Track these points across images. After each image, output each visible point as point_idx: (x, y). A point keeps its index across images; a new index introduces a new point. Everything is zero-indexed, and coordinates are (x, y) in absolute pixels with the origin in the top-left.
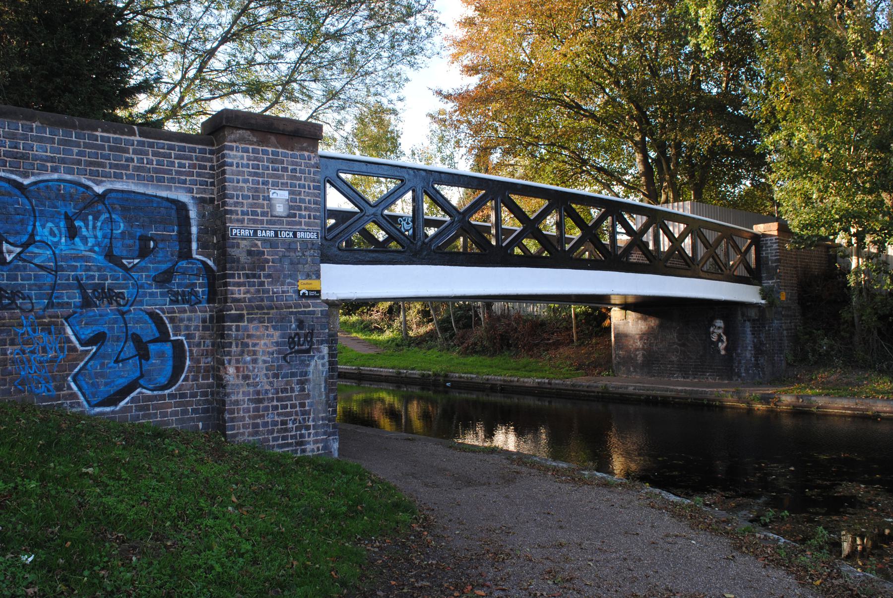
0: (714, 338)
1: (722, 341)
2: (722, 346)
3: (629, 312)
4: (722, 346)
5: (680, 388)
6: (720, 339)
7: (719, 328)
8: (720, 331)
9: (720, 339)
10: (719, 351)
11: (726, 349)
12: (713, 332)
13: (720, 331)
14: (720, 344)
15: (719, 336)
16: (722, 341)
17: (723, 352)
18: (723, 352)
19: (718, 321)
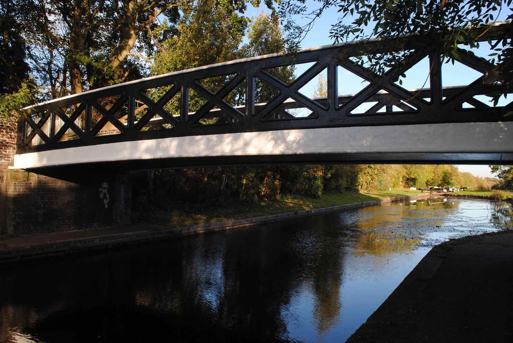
0: (101, 196)
1: (106, 198)
2: (106, 201)
3: (32, 174)
4: (106, 201)
5: (131, 233)
6: (105, 197)
7: (105, 188)
8: (106, 191)
9: (105, 197)
10: (104, 205)
11: (108, 204)
12: (101, 192)
13: (106, 191)
14: (105, 200)
15: (105, 194)
16: (106, 198)
17: (106, 206)
18: (106, 206)
19: (104, 183)
